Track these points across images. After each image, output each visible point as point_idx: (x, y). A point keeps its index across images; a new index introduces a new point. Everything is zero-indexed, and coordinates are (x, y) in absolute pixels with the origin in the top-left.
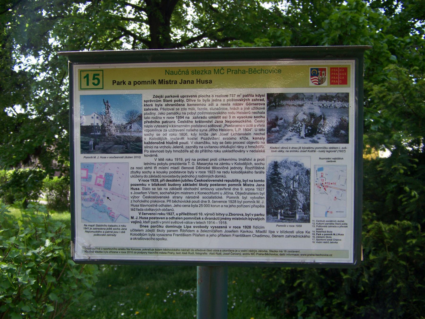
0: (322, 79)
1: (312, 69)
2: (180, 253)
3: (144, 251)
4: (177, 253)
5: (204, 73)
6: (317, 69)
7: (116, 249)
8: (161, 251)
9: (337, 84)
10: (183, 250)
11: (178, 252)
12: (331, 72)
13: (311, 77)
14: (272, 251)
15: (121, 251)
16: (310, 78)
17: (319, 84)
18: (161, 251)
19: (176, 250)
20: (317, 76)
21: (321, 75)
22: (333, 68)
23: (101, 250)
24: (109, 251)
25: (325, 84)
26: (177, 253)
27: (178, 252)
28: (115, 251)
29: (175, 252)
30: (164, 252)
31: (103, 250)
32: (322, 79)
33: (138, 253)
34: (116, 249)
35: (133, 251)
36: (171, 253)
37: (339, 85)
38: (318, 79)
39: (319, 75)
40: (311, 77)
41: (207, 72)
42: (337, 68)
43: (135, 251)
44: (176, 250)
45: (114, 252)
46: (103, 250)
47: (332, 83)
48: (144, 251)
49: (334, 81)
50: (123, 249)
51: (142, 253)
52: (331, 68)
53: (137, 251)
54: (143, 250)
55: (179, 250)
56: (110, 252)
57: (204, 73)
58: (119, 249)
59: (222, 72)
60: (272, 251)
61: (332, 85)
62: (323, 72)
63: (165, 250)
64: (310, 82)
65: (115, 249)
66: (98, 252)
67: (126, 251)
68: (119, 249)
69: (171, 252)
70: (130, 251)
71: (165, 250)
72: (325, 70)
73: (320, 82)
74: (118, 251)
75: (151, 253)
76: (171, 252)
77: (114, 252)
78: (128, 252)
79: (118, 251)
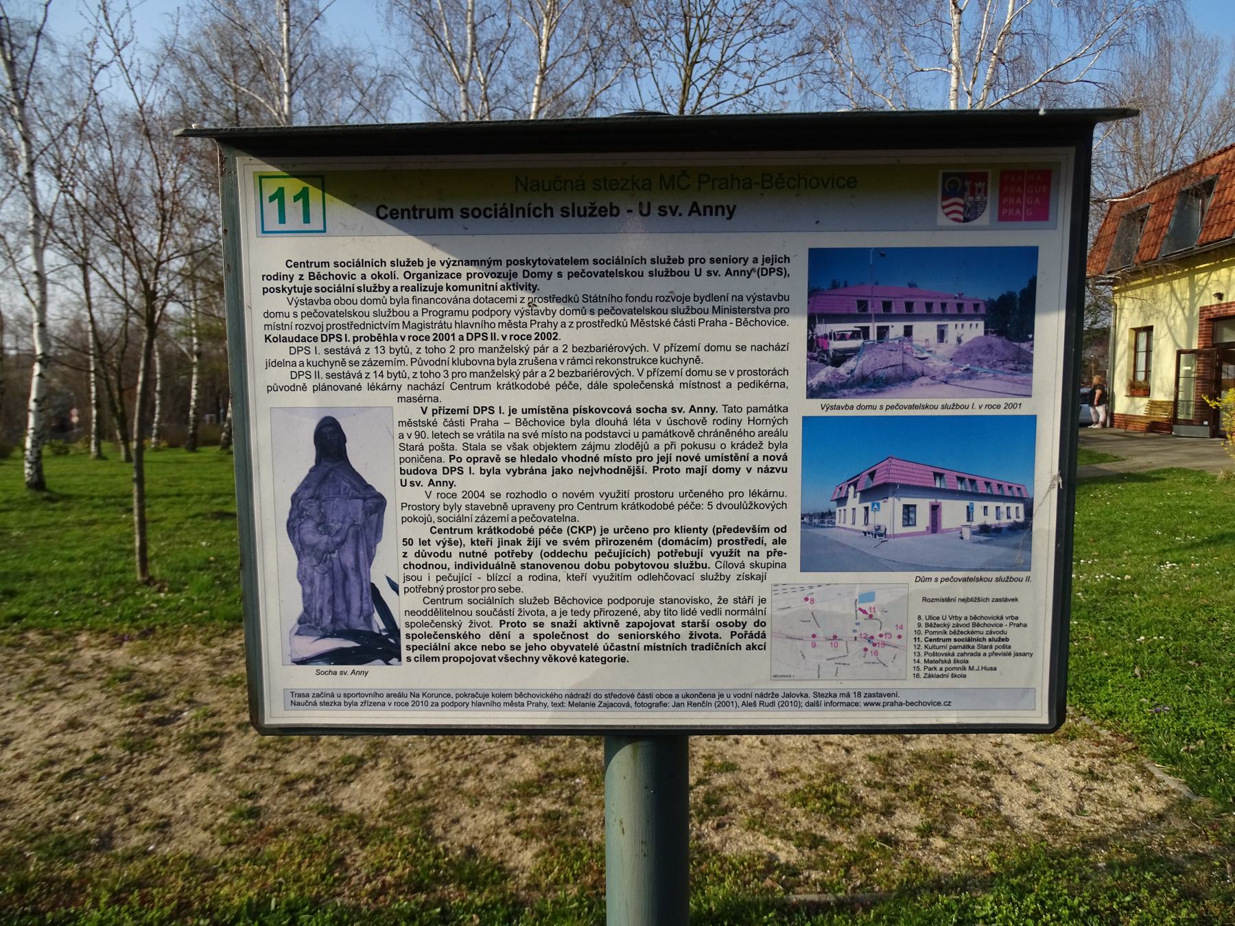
0: (975, 204)
1: (946, 176)
3: (460, 700)
4: (554, 705)
7: (381, 695)
8: (508, 700)
9: (1018, 218)
11: (556, 700)
13: (945, 198)
15: (393, 700)
17: (966, 220)
18: (508, 700)
19: (552, 696)
20: (962, 197)
21: (973, 194)
23: (336, 699)
24: (359, 700)
25: (985, 219)
27: (556, 700)
29: (548, 701)
30: (516, 700)
31: (342, 700)
32: (975, 204)
33: (444, 704)
34: (381, 695)
35: (430, 700)
36: (537, 705)
37: (1024, 223)
38: (964, 206)
39: (967, 194)
40: (945, 198)
43: (434, 699)
44: (552, 696)
45: (375, 704)
46: (342, 700)
47: (1002, 218)
48: (460, 700)
49: (1011, 212)
50: (400, 695)
51: (454, 704)
53: (440, 700)
54: (458, 696)
55: (560, 696)
56: (363, 704)
58: (389, 696)
61: (1003, 224)
62: (979, 185)
63: (521, 695)
64: (941, 213)
65: (376, 695)
66: (327, 704)
67: (409, 700)
68: (389, 696)
69: (536, 700)
70: (420, 699)
71: (521, 695)
74: (385, 699)
75: (480, 704)
76: (536, 700)
77: (375, 704)
78: (415, 704)
79: (385, 699)
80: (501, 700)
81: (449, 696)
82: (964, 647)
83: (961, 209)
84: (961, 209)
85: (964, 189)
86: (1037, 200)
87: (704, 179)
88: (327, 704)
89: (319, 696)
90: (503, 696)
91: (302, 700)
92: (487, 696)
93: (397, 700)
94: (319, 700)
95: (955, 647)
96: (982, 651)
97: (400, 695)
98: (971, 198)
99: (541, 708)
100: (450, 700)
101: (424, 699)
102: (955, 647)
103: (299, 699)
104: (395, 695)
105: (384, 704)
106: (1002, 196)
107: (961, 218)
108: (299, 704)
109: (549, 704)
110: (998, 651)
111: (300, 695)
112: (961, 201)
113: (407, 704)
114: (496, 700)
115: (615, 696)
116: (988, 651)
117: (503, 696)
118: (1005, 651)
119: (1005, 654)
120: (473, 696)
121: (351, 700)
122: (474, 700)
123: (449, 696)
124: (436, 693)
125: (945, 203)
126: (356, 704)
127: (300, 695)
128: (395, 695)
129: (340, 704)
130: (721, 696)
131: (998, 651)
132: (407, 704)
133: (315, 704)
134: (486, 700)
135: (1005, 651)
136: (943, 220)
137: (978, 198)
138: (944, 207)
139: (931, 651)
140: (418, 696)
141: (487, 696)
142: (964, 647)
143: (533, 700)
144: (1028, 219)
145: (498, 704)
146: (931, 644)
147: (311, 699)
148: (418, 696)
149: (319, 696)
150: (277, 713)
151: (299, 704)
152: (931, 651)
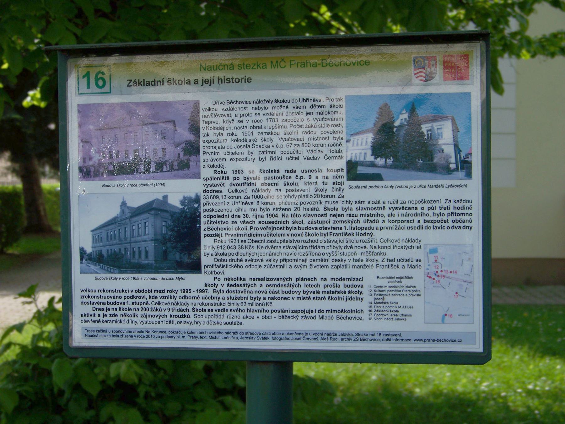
3: (171, 335)
7: (131, 332)
13: (415, 70)
15: (137, 334)
17: (427, 81)
23: (108, 334)
24: (119, 334)
28: (129, 334)
31: (111, 334)
33: (163, 337)
34: (131, 332)
35: (156, 334)
40: (415, 70)
45: (128, 336)
46: (111, 334)
48: (171, 335)
50: (140, 332)
51: (167, 337)
53: (161, 335)
54: (170, 332)
56: (122, 336)
58: (135, 332)
66: (103, 336)
67: (145, 334)
68: (135, 332)
70: (151, 334)
73: (428, 79)
74: (133, 334)
77: (128, 336)
79: (133, 334)
81: (165, 332)
82: (395, 291)
83: (424, 75)
84: (424, 75)
88: (103, 336)
89: (99, 331)
91: (91, 334)
93: (139, 334)
94: (99, 334)
95: (390, 291)
96: (405, 293)
97: (140, 332)
98: (428, 69)
100: (165, 335)
102: (390, 291)
103: (89, 334)
104: (138, 332)
105: (132, 337)
107: (424, 79)
108: (89, 336)
110: (414, 293)
111: (90, 331)
112: (424, 71)
113: (144, 337)
116: (408, 293)
118: (417, 293)
119: (417, 295)
121: (115, 334)
123: (165, 332)
124: (159, 331)
127: (90, 331)
128: (138, 332)
131: (414, 293)
132: (144, 337)
133: (97, 336)
135: (417, 293)
138: (415, 74)
139: (377, 293)
142: (395, 291)
146: (377, 289)
147: (95, 333)
149: (99, 331)
151: (89, 336)
152: (377, 293)
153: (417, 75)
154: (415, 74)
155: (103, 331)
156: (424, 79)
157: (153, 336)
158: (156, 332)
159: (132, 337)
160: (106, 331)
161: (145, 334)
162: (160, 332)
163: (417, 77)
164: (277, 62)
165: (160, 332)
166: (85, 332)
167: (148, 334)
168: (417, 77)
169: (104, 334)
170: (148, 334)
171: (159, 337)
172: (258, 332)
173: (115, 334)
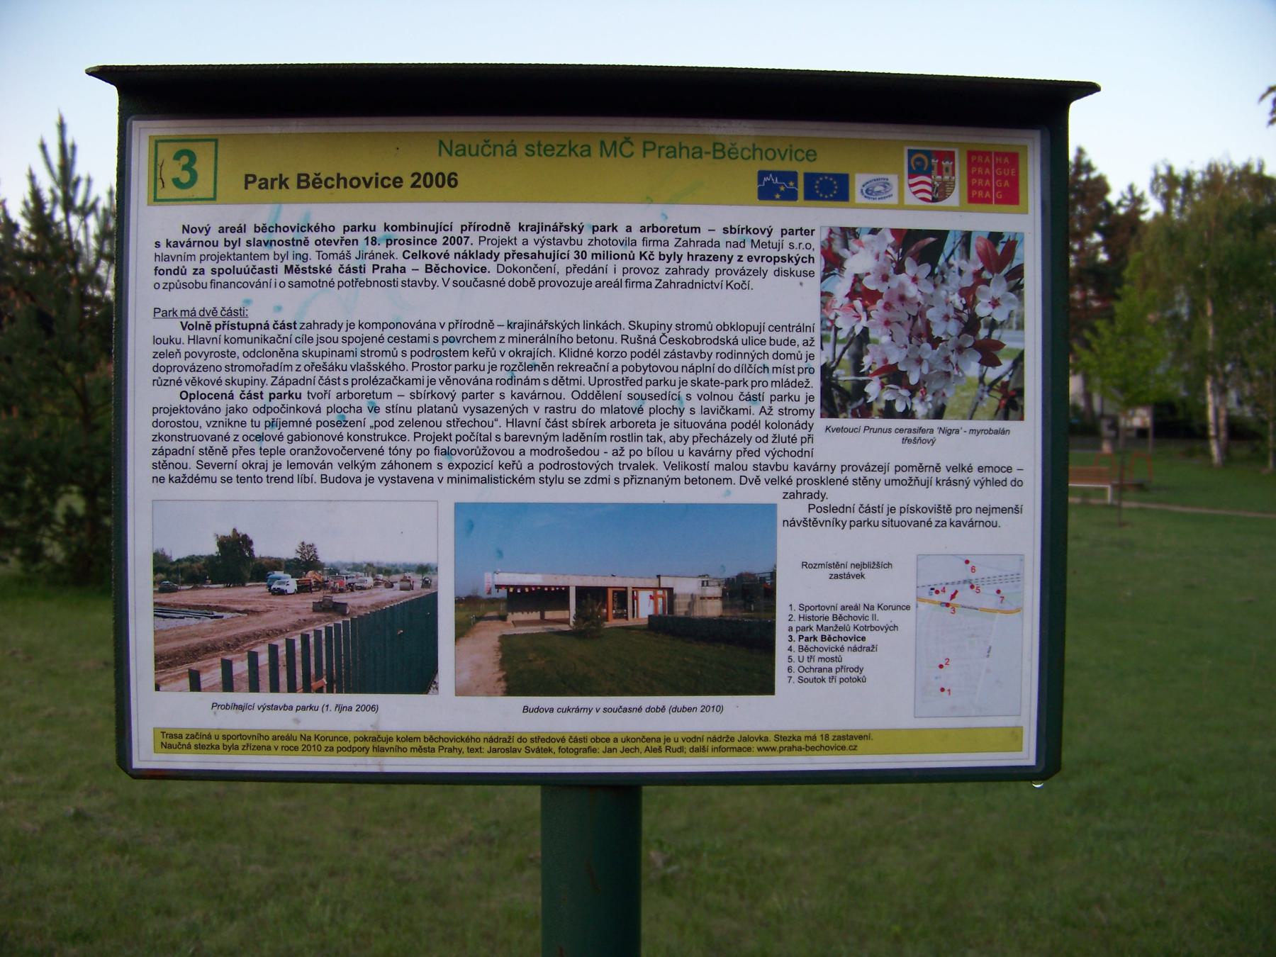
0: (943, 184)
1: (911, 153)
2: (479, 750)
3: (358, 744)
5: (566, 151)
6: (929, 154)
8: (416, 744)
9: (988, 201)
10: (491, 740)
11: (473, 745)
12: (970, 164)
13: (911, 176)
14: (784, 739)
15: (280, 743)
16: (906, 181)
17: (934, 200)
18: (416, 744)
19: (468, 740)
20: (930, 176)
21: (940, 173)
22: (976, 153)
23: (214, 742)
24: (240, 743)
25: (954, 199)
26: (471, 750)
27: (473, 745)
29: (463, 746)
30: (425, 745)
31: (221, 742)
32: (943, 184)
33: (340, 749)
34: (266, 738)
35: (324, 744)
36: (451, 750)
37: (993, 206)
38: (931, 185)
39: (935, 172)
40: (911, 176)
41: (578, 150)
42: (989, 153)
43: (328, 743)
44: (468, 740)
45: (259, 748)
47: (972, 200)
48: (358, 744)
49: (980, 194)
50: (289, 738)
51: (352, 750)
52: (970, 154)
53: (335, 744)
54: (356, 739)
55: (477, 740)
57: (566, 151)
58: (275, 738)
59: (626, 152)
60: (784, 739)
62: (946, 164)
63: (431, 739)
64: (908, 192)
65: (260, 736)
66: (203, 747)
67: (299, 743)
68: (275, 738)
69: (449, 745)
70: (312, 742)
72: (951, 156)
73: (939, 194)
74: (271, 743)
76: (449, 745)
77: (259, 748)
79: (271, 743)
80: (408, 745)
81: (345, 739)
83: (929, 189)
84: (929, 189)
85: (931, 167)
86: (1007, 184)
87: (650, 146)
89: (193, 737)
90: (410, 739)
91: (175, 742)
92: (390, 739)
94: (193, 742)
98: (939, 177)
99: (455, 754)
100: (346, 744)
101: (317, 742)
103: (170, 740)
104: (282, 738)
105: (269, 748)
106: (970, 176)
107: (929, 197)
108: (170, 746)
109: (465, 750)
111: (171, 736)
112: (929, 180)
113: (296, 748)
114: (402, 745)
115: (543, 740)
117: (410, 739)
120: (375, 739)
121: (230, 743)
122: (376, 744)
123: (345, 739)
125: (913, 181)
126: (237, 748)
127: (171, 736)
128: (282, 738)
129: (218, 747)
130: (668, 740)
132: (296, 748)
133: (189, 747)
134: (390, 744)
136: (910, 199)
137: (946, 178)
138: (911, 186)
140: (309, 738)
141: (390, 739)
143: (445, 745)
144: (998, 202)
145: (404, 750)
147: (184, 741)
148: (309, 738)
149: (193, 737)
150: (145, 755)
151: (170, 746)
153: (915, 189)
154: (911, 186)
155: (202, 736)
156: (929, 197)
157: (318, 748)
158: (326, 739)
159: (269, 748)
160: (209, 737)
161: (299, 743)
162: (333, 739)
163: (915, 193)
164: (615, 143)
165: (333, 739)
166: (160, 738)
167: (306, 743)
168: (915, 193)
169: (205, 742)
170: (306, 743)
171: (332, 749)
172: (560, 736)
173: (230, 743)
